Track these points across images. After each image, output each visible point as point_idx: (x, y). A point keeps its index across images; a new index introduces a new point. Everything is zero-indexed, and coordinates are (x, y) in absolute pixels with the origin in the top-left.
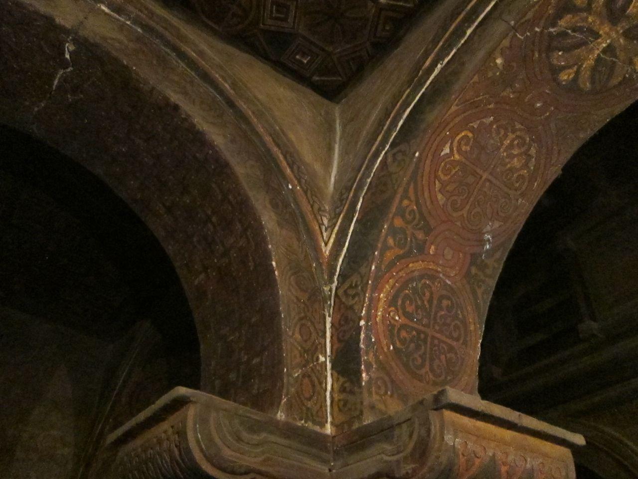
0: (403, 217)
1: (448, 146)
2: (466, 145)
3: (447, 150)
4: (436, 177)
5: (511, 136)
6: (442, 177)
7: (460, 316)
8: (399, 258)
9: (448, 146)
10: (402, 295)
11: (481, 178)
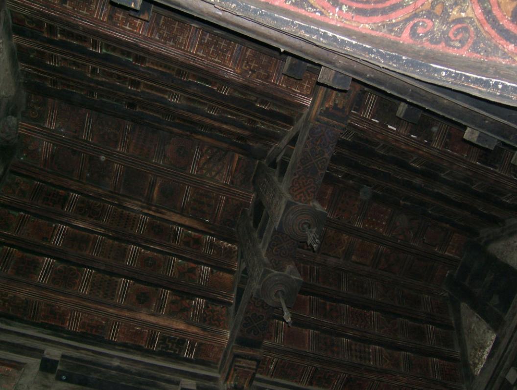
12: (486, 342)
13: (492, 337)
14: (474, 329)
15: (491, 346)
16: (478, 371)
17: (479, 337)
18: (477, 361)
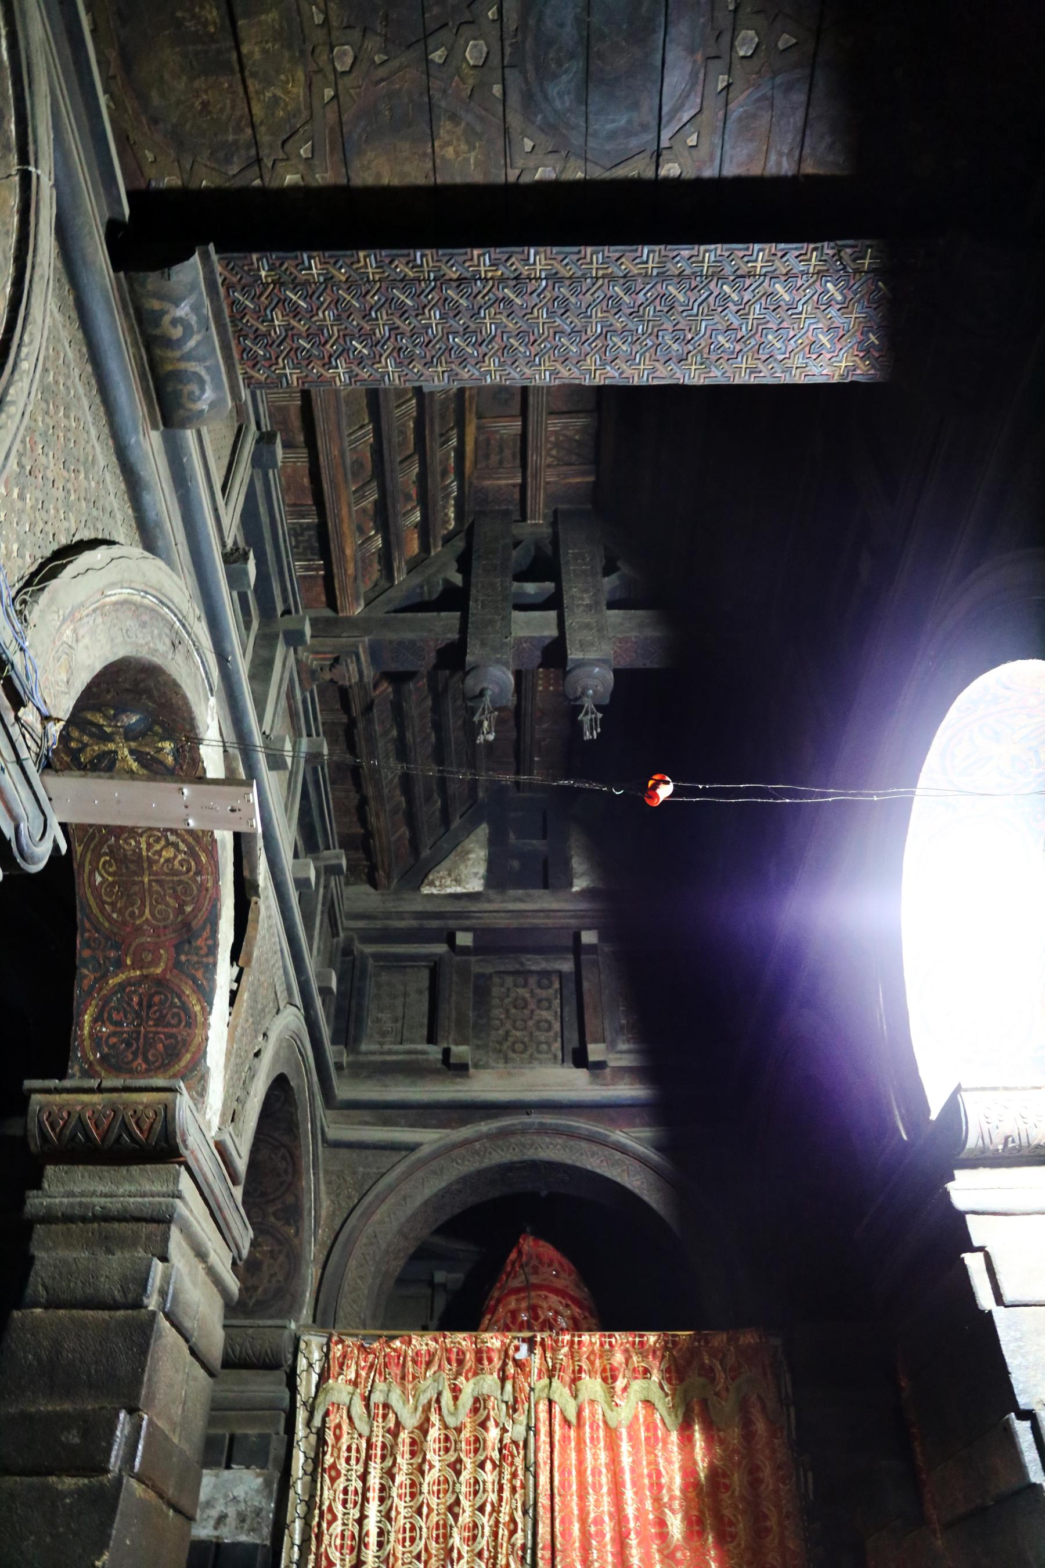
0: (89, 947)
1: (97, 875)
2: (111, 866)
3: (99, 879)
4: (104, 902)
5: (143, 840)
6: (109, 900)
7: (179, 1004)
8: (96, 980)
9: (97, 875)
10: (107, 1009)
11: (143, 882)
12: (467, 883)
13: (476, 885)
14: (469, 859)
15: (464, 891)
16: (426, 890)
17: (466, 872)
18: (437, 883)
